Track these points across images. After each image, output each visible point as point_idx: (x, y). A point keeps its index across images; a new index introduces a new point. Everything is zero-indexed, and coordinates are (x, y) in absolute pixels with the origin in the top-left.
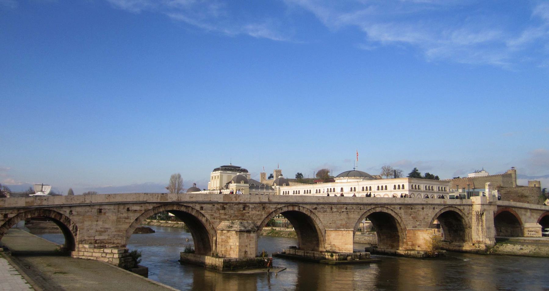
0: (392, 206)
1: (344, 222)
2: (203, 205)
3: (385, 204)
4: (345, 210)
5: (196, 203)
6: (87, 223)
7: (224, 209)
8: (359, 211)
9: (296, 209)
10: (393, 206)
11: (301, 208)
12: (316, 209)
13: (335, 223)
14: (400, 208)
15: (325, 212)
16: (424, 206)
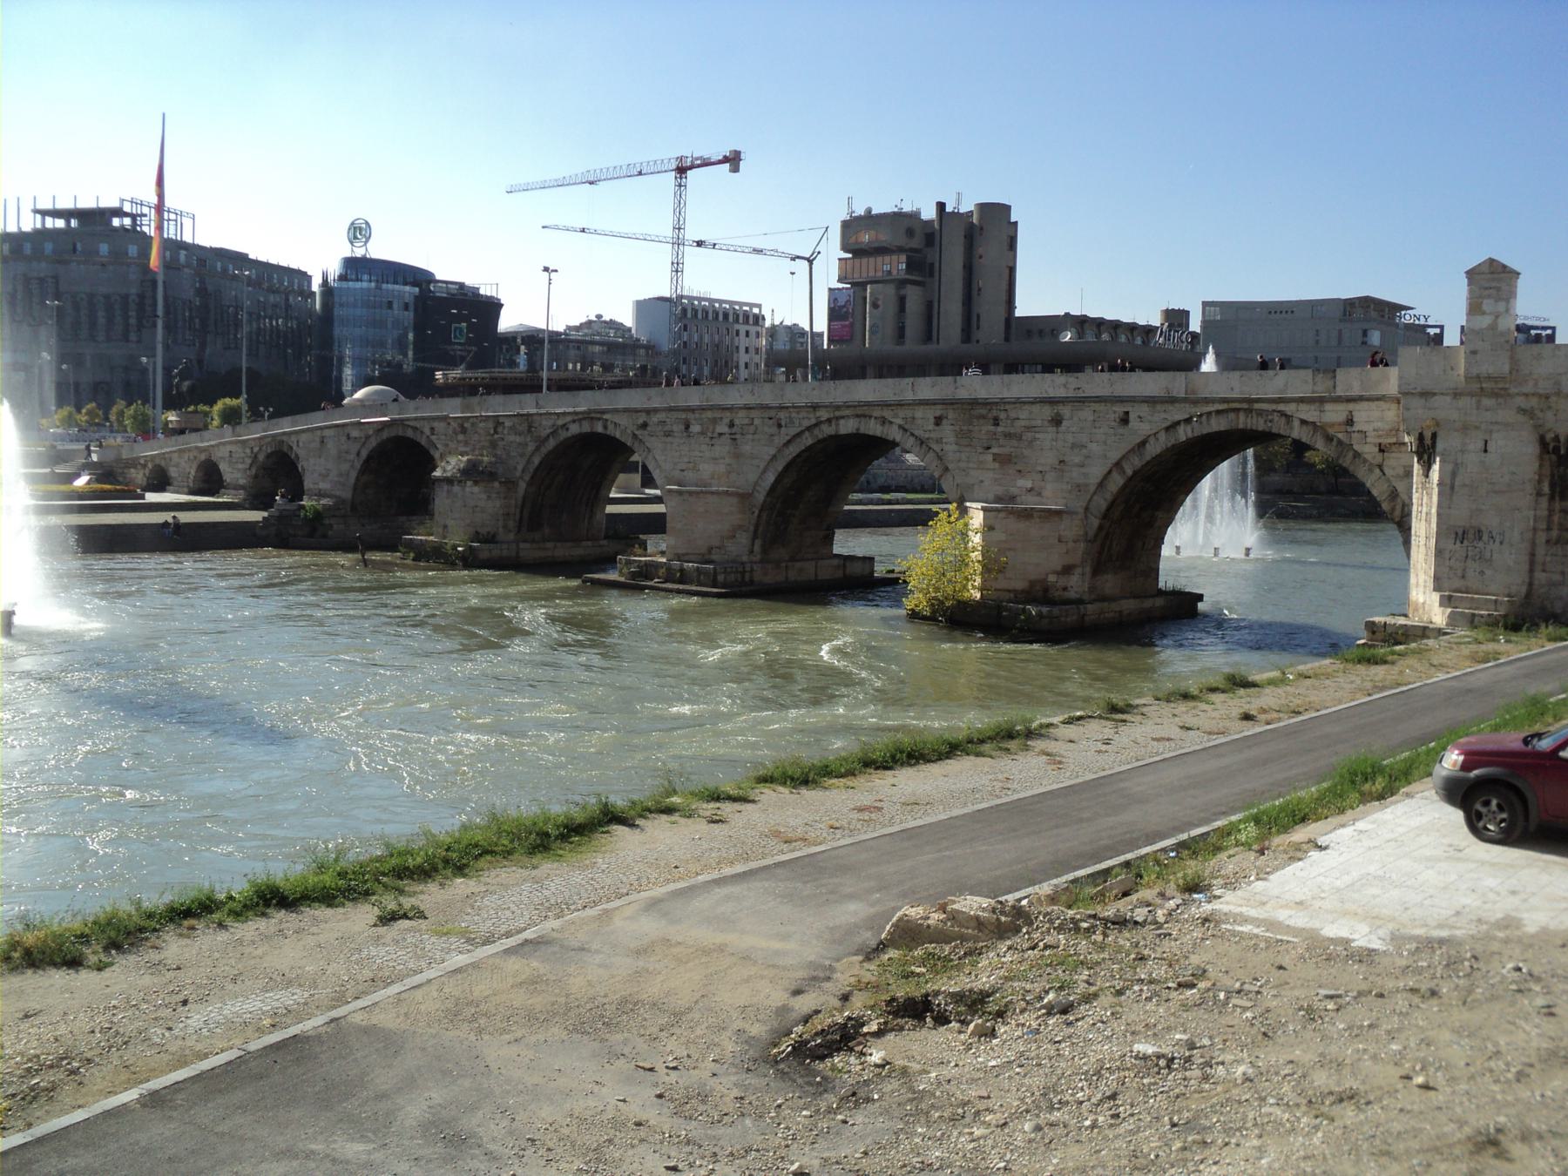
0: (902, 413)
1: (722, 468)
2: (436, 424)
3: (868, 404)
4: (725, 429)
5: (423, 419)
6: (312, 461)
7: (464, 431)
8: (774, 430)
9: (599, 429)
10: (907, 412)
11: (611, 427)
12: (644, 426)
13: (695, 469)
14: (938, 421)
15: (668, 434)
16: (1065, 411)
